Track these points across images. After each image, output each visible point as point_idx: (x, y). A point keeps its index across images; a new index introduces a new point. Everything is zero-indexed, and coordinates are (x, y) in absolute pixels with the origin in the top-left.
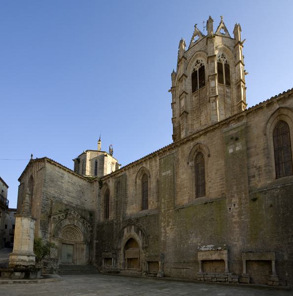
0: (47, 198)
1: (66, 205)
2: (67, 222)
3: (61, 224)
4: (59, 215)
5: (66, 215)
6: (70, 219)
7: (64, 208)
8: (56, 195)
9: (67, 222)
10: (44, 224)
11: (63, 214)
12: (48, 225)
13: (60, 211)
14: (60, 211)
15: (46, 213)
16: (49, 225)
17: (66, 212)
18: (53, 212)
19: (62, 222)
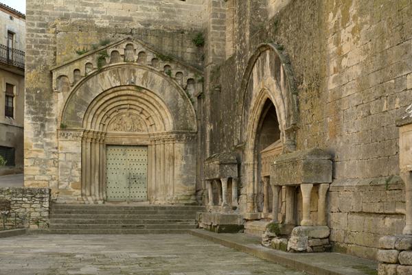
0: (40, 25)
1: (101, 31)
2: (107, 81)
3: (87, 90)
4: (76, 65)
5: (101, 59)
6: (115, 71)
7: (94, 40)
8: (71, 9)
9: (107, 81)
10: (39, 98)
11: (90, 60)
12: (49, 98)
13: (80, 53)
14: (80, 53)
15: (42, 66)
16: (54, 97)
17: (102, 56)
18: (59, 60)
19: (90, 83)
